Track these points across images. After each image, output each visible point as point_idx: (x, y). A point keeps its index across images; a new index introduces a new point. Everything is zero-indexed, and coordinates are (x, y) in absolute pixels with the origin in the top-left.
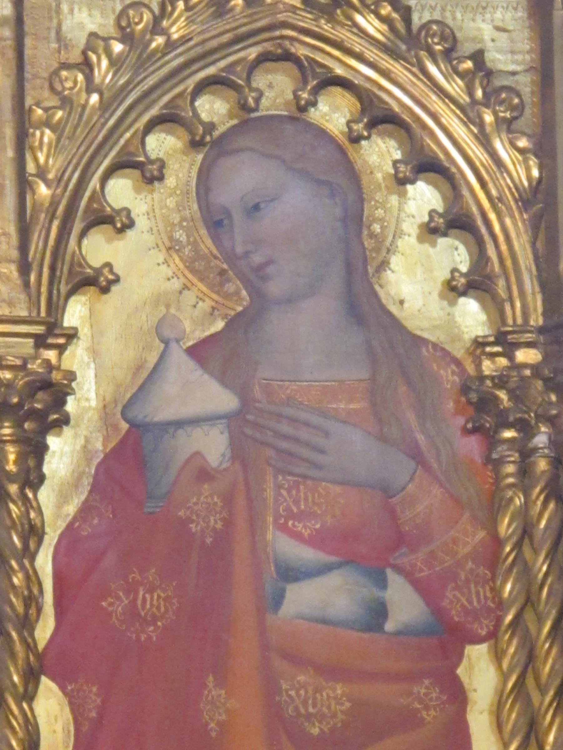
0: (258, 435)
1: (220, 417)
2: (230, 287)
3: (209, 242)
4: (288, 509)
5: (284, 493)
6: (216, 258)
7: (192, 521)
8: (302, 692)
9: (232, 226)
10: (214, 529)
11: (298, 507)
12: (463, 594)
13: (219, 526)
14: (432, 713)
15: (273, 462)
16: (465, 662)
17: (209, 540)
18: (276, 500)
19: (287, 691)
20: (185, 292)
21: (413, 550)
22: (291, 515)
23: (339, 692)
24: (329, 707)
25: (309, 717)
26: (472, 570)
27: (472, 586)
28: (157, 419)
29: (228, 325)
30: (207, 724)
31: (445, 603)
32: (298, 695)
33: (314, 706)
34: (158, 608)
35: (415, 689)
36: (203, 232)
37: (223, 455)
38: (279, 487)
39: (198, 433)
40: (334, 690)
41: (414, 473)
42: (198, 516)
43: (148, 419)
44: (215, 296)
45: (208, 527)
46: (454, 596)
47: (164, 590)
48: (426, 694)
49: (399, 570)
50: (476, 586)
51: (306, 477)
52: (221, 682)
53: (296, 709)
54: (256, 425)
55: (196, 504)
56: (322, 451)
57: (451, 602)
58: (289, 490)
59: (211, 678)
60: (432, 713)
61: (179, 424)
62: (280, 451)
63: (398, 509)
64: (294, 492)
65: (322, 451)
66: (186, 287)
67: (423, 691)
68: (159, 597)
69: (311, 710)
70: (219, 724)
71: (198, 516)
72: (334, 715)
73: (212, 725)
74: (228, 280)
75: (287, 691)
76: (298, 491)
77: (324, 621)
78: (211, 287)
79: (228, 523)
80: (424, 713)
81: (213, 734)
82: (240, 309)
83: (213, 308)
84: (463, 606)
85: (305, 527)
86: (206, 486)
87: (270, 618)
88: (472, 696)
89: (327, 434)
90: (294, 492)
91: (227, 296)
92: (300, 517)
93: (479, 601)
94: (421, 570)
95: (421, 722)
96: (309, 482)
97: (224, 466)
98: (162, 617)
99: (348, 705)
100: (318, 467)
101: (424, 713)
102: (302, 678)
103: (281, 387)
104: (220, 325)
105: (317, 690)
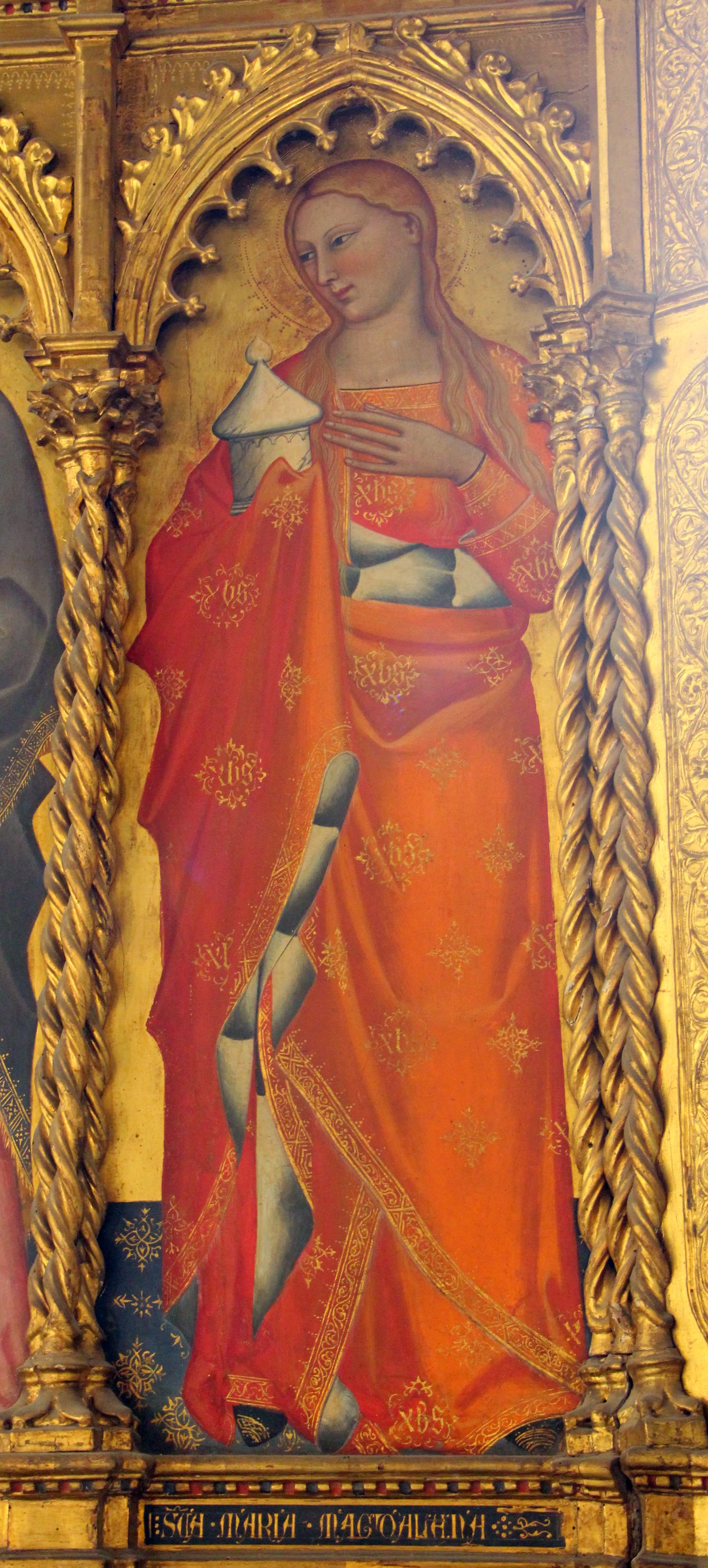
0: (336, 439)
1: (303, 426)
2: (314, 312)
3: (295, 274)
4: (363, 502)
5: (360, 488)
6: (300, 287)
7: (275, 519)
8: (374, 666)
9: (316, 257)
10: (295, 524)
11: (372, 499)
12: (528, 568)
13: (299, 521)
14: (498, 678)
15: (349, 461)
16: (529, 629)
17: (289, 535)
18: (352, 495)
19: (359, 665)
20: (274, 319)
21: (480, 531)
22: (365, 507)
23: (409, 663)
24: (399, 678)
25: (379, 688)
26: (536, 545)
27: (537, 560)
28: (244, 432)
29: (311, 345)
30: (284, 699)
31: (512, 577)
32: (370, 669)
33: (385, 677)
34: (242, 598)
35: (482, 657)
36: (290, 266)
37: (304, 459)
38: (354, 483)
39: (282, 440)
40: (404, 662)
41: (482, 462)
42: (280, 514)
43: (236, 432)
44: (299, 321)
45: (288, 523)
46: (520, 570)
47: (247, 582)
48: (492, 661)
49: (465, 549)
50: (541, 557)
51: (381, 473)
52: (296, 663)
53: (368, 680)
54: (334, 429)
55: (278, 503)
56: (396, 448)
57: (516, 576)
58: (364, 485)
59: (288, 658)
60: (498, 678)
61: (265, 434)
62: (356, 451)
63: (466, 495)
64: (369, 487)
65: (396, 448)
66: (273, 315)
67: (489, 658)
68: (242, 588)
69: (381, 681)
70: (295, 698)
71: (280, 514)
72: (404, 686)
73: (289, 700)
74: (312, 306)
75: (359, 665)
76: (373, 486)
77: (395, 600)
78: (296, 313)
79: (308, 518)
80: (489, 679)
81: (290, 708)
82: (322, 330)
83: (298, 331)
84: (527, 578)
85: (378, 516)
86: (288, 487)
87: (344, 599)
88: (535, 660)
89: (400, 433)
90: (369, 487)
91: (310, 320)
92: (374, 508)
93: (543, 572)
94: (488, 549)
95: (487, 687)
96: (383, 477)
97: (305, 468)
98: (245, 604)
99: (417, 675)
100: (391, 462)
101: (489, 679)
102: (374, 653)
103: (357, 394)
104: (304, 345)
105: (389, 662)
